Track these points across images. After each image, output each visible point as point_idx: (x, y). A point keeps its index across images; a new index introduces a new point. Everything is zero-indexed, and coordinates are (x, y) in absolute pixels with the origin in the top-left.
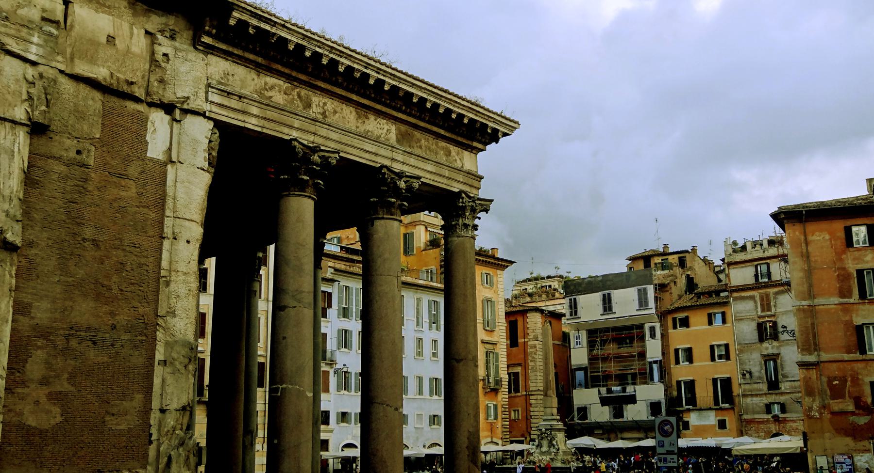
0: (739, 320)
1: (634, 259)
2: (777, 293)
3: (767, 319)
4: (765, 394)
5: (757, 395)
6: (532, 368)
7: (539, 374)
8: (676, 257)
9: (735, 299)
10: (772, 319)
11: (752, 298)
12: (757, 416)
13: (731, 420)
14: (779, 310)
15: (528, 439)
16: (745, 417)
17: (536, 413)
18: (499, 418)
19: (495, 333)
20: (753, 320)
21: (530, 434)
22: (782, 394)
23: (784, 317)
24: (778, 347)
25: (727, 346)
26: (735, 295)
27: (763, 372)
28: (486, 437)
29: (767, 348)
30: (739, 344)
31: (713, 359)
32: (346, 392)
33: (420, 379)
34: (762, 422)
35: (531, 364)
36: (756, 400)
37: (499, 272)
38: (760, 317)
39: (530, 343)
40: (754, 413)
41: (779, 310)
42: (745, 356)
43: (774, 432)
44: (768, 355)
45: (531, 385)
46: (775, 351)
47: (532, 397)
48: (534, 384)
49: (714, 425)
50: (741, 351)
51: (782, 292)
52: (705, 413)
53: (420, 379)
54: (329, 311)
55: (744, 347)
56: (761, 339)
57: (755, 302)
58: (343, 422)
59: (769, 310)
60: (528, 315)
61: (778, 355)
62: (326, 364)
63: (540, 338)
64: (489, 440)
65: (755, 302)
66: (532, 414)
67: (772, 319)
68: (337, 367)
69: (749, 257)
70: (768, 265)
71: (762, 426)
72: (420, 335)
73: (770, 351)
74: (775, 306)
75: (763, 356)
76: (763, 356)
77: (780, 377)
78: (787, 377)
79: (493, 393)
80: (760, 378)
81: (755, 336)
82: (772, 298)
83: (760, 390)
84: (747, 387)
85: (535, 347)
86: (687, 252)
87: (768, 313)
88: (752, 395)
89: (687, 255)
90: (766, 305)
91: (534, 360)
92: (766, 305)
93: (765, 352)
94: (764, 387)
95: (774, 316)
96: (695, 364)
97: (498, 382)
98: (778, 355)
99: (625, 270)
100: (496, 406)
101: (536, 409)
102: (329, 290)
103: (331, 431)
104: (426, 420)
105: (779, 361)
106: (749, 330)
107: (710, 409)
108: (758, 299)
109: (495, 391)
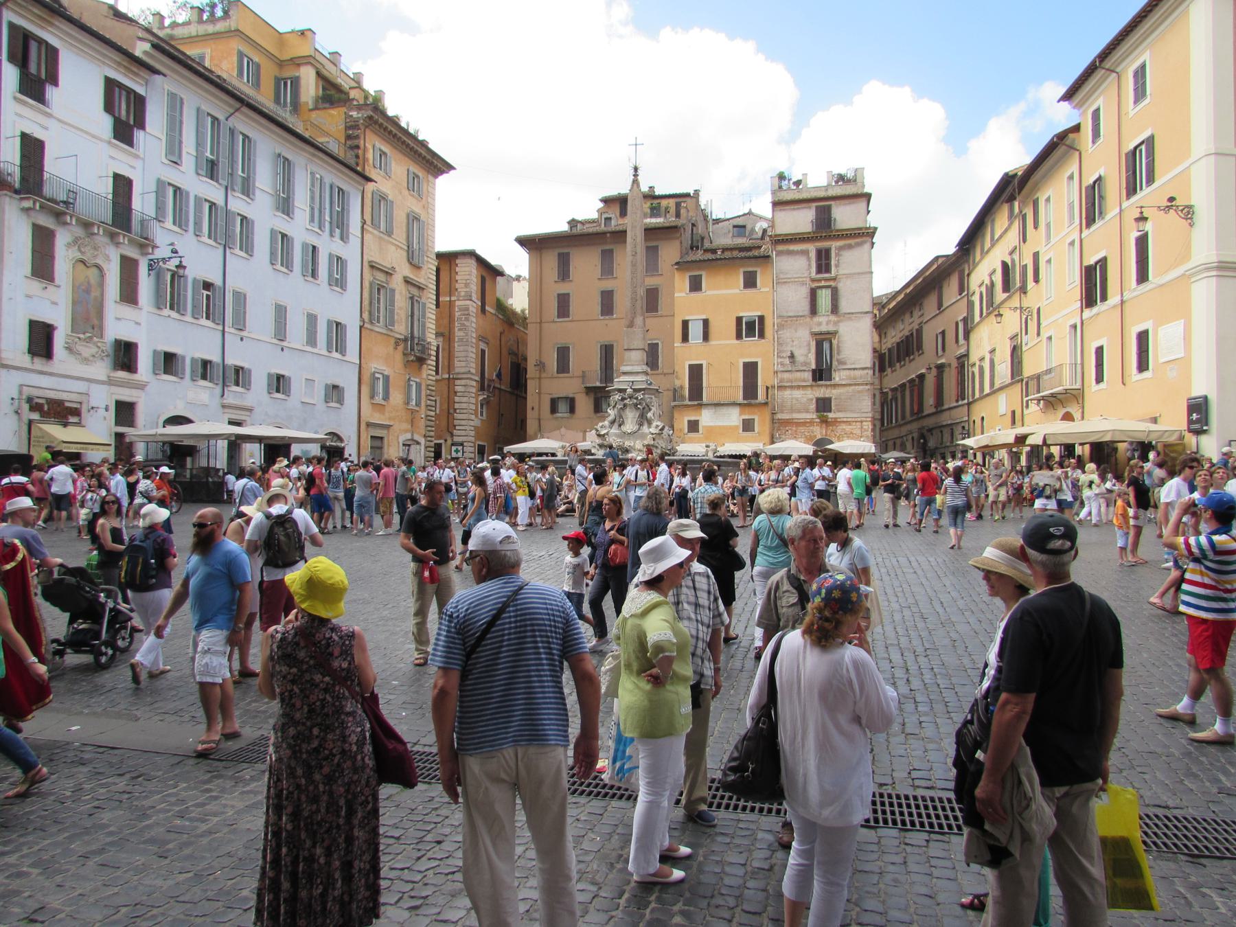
0: (780, 282)
1: (607, 201)
2: (841, 248)
3: (823, 283)
4: (811, 386)
5: (799, 387)
6: (461, 340)
7: (470, 349)
8: (672, 202)
9: (779, 253)
10: (832, 283)
11: (805, 253)
12: (795, 416)
13: (761, 421)
14: (841, 272)
15: (449, 442)
16: (779, 416)
17: (464, 406)
18: (423, 404)
19: (423, 272)
20: (803, 284)
21: (452, 435)
22: (835, 386)
23: (848, 282)
24: (836, 323)
25: (761, 318)
26: (780, 248)
27: (812, 358)
28: (406, 431)
29: (820, 324)
30: (779, 317)
31: (739, 336)
32: (174, 314)
33: (312, 319)
34: (804, 424)
35: (458, 334)
36: (797, 394)
37: (431, 178)
38: (813, 280)
39: (458, 303)
40: (792, 411)
41: (841, 272)
42: (786, 334)
43: (819, 437)
44: (821, 334)
45: (457, 364)
46: (831, 328)
47: (457, 382)
48: (463, 364)
49: (737, 427)
50: (781, 326)
51: (850, 247)
52: (724, 410)
53: (312, 319)
54: (139, 135)
55: (787, 321)
56: (814, 310)
57: (809, 259)
58: (165, 372)
59: (828, 270)
60: (458, 261)
61: (835, 333)
62: (131, 241)
63: (474, 297)
64: (409, 436)
65: (809, 259)
66: (457, 406)
67: (832, 283)
68: (159, 254)
69: (805, 195)
70: (829, 208)
71: (802, 429)
72: (313, 240)
73: (824, 328)
74: (837, 266)
75: (814, 334)
76: (814, 334)
77: (835, 363)
78: (845, 363)
79: (416, 364)
80: (806, 364)
81: (805, 307)
82: (833, 255)
83: (804, 381)
84: (786, 376)
85: (467, 309)
86: (687, 195)
87: (826, 275)
88: (792, 387)
89: (688, 200)
90: (823, 261)
91: (463, 328)
92: (823, 261)
93: (816, 329)
94: (808, 376)
95: (834, 279)
96: (712, 342)
97: (425, 348)
98: (835, 333)
99: (595, 216)
100: (419, 385)
101: (465, 399)
102: (140, 90)
103: (141, 386)
104: (320, 393)
105: (835, 342)
106: (796, 298)
107: (734, 404)
108: (813, 255)
109: (421, 361)
